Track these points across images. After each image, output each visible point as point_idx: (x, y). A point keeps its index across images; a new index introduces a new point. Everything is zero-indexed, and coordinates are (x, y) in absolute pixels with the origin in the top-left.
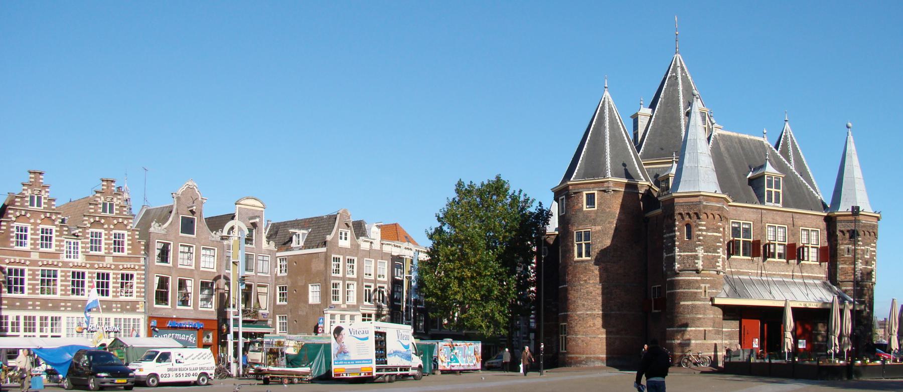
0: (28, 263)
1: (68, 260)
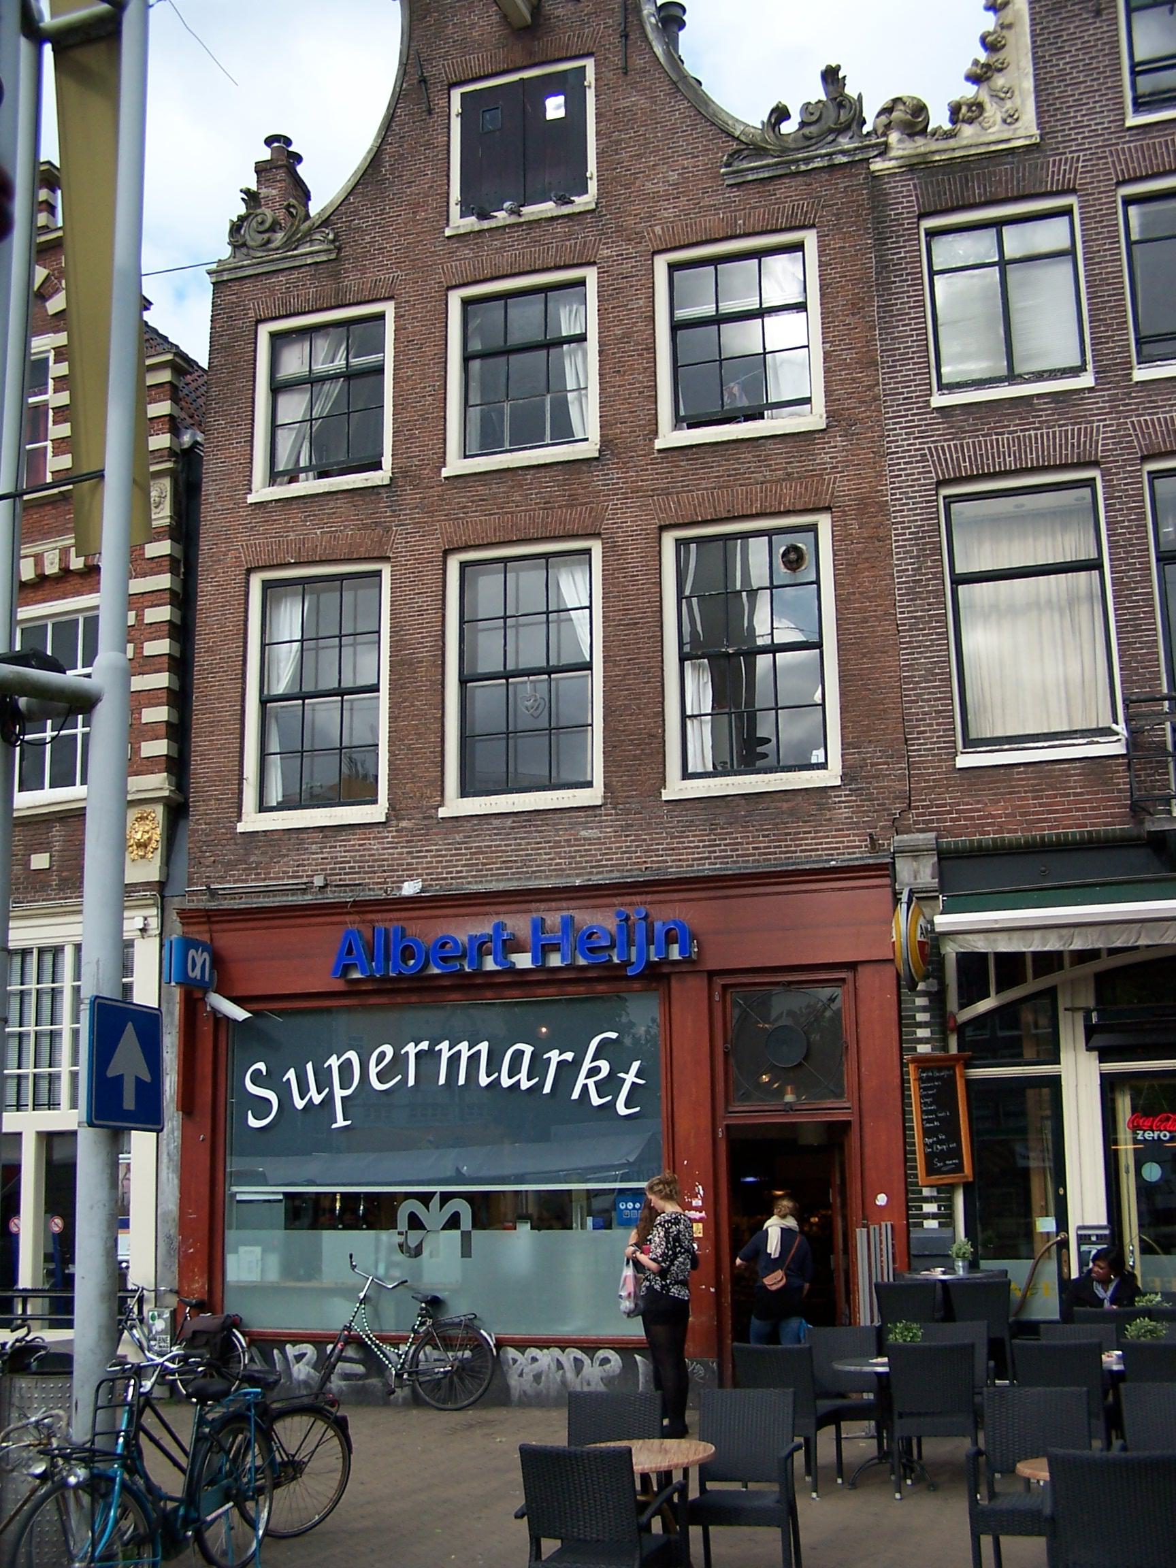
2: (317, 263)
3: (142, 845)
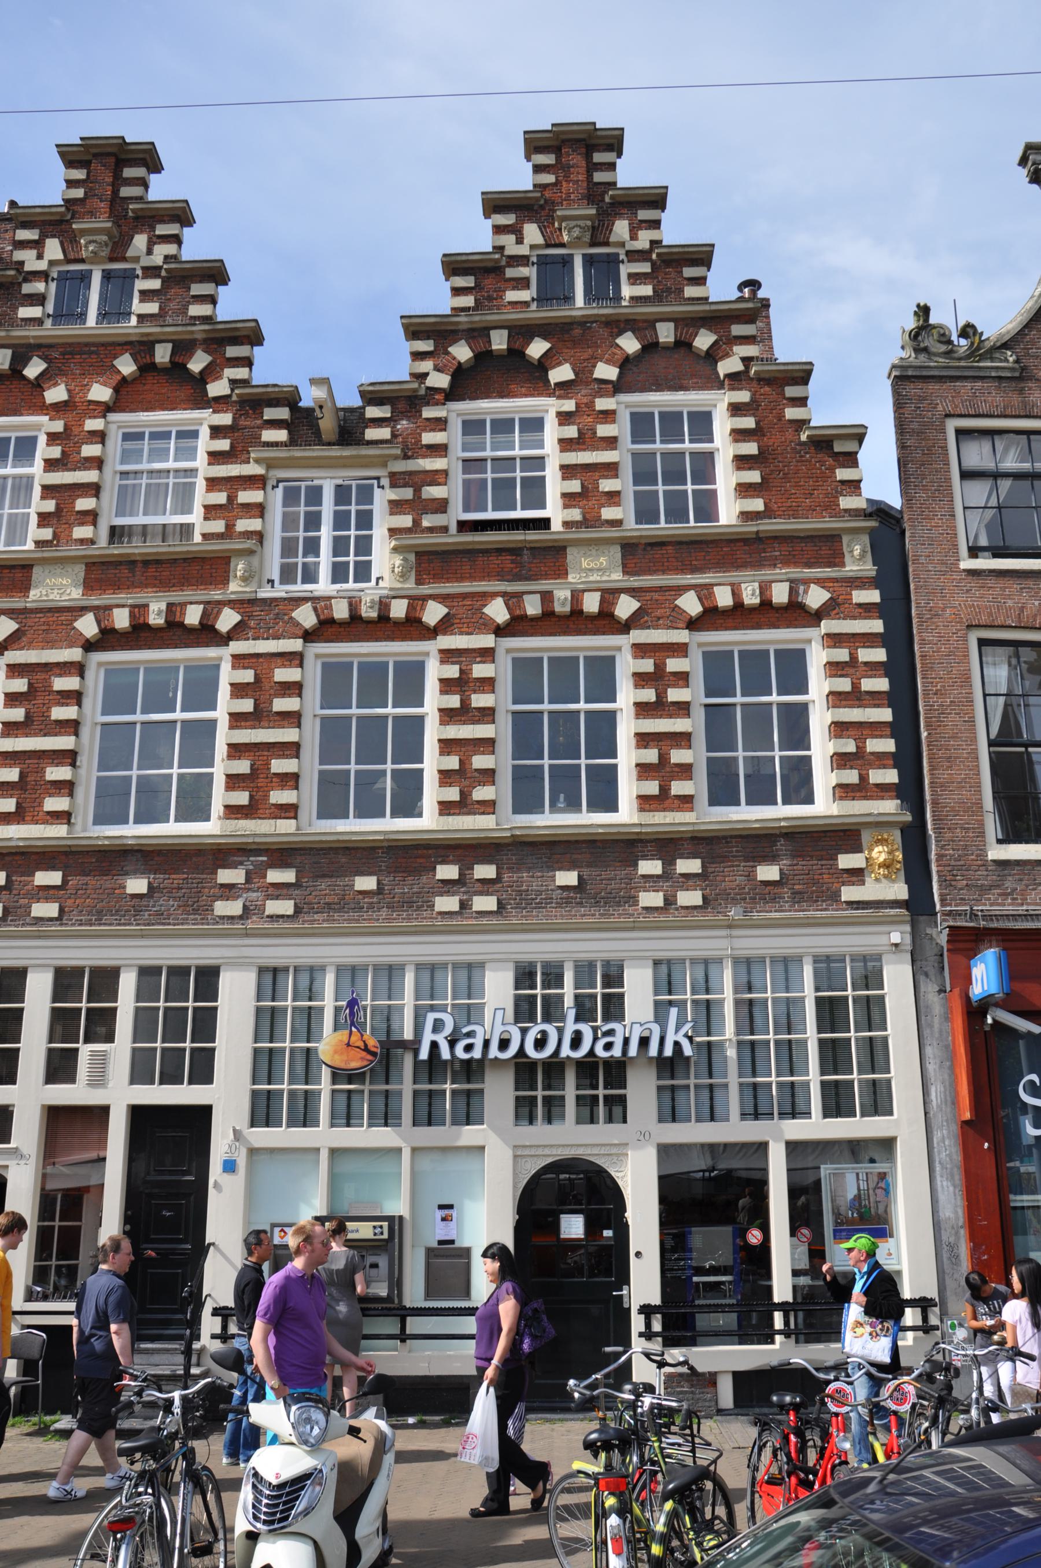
1: (299, 588)
2: (1000, 378)
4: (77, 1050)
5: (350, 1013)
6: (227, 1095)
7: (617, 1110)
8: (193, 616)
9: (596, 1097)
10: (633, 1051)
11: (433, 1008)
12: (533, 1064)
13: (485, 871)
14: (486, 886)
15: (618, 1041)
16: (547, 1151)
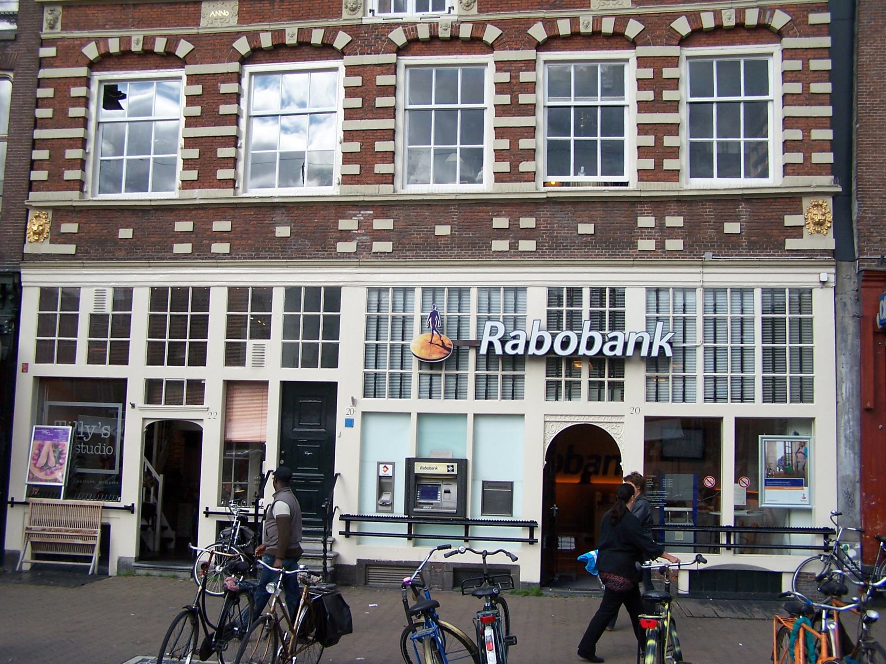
0: (183, 49)
1: (392, 15)
3: (820, 224)
4: (245, 343)
5: (434, 320)
6: (348, 375)
7: (617, 393)
8: (317, 38)
9: (603, 383)
10: (630, 352)
11: (489, 319)
12: (560, 359)
13: (527, 222)
14: (528, 234)
15: (620, 344)
16: (567, 419)
